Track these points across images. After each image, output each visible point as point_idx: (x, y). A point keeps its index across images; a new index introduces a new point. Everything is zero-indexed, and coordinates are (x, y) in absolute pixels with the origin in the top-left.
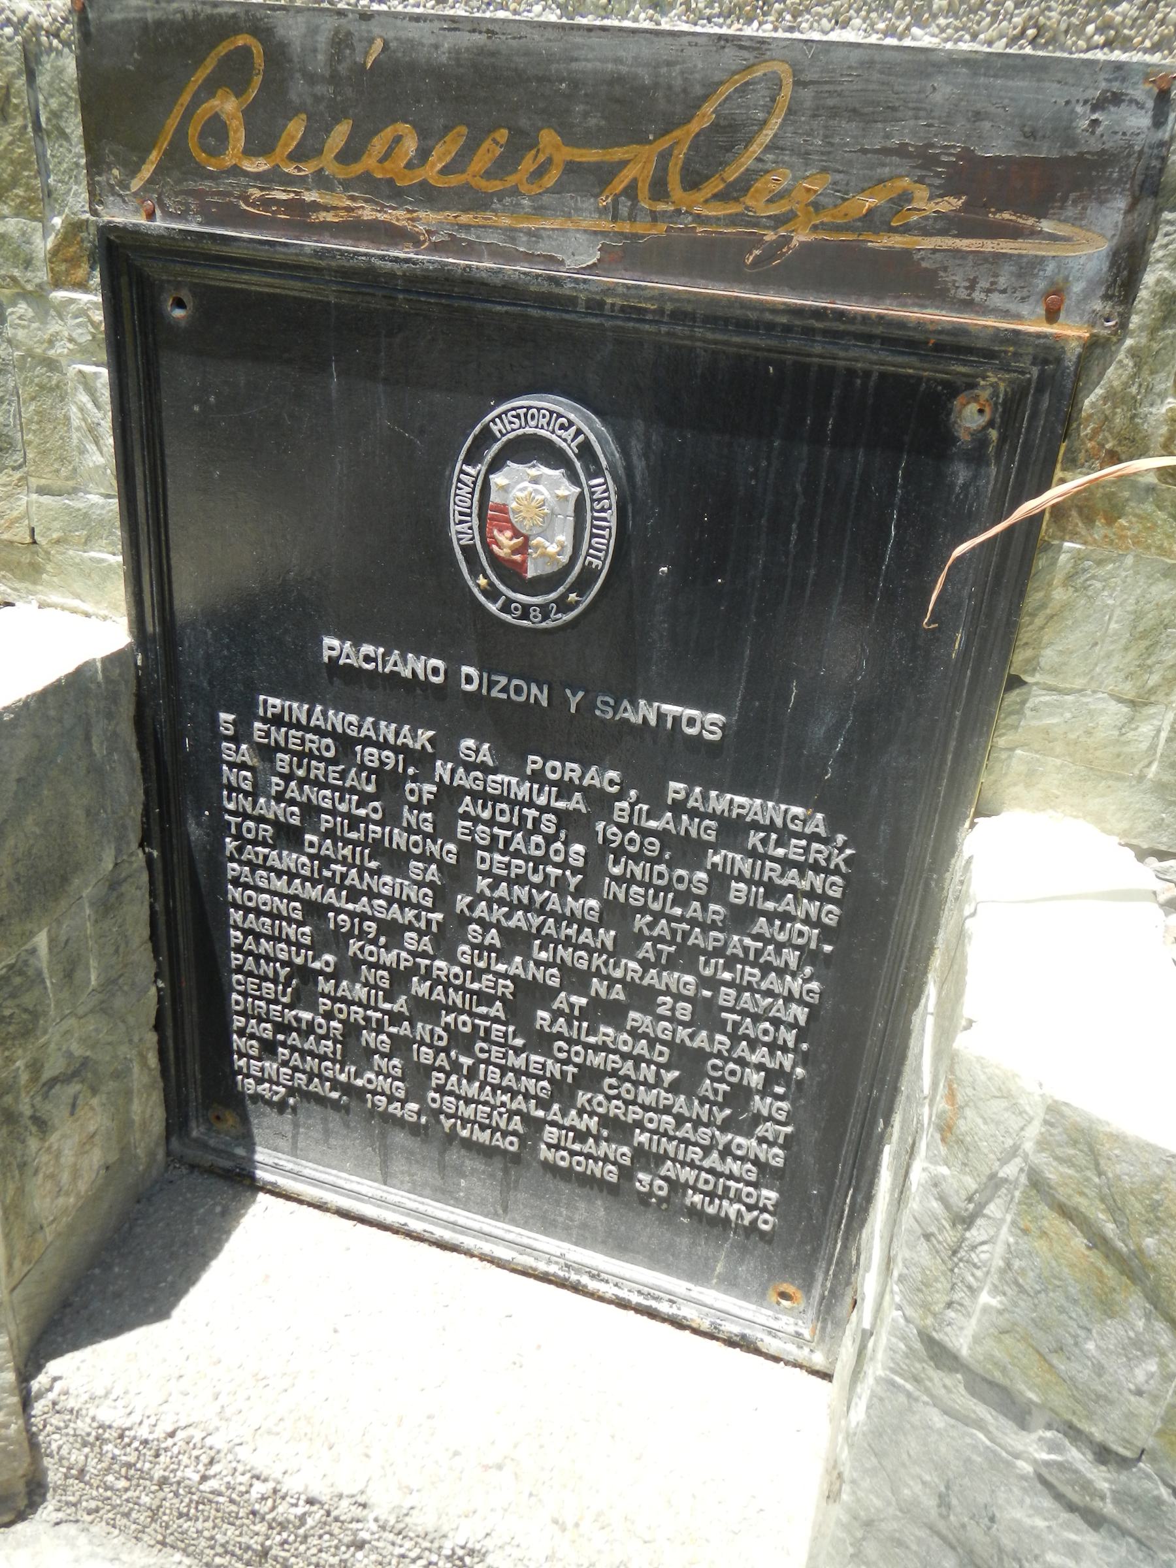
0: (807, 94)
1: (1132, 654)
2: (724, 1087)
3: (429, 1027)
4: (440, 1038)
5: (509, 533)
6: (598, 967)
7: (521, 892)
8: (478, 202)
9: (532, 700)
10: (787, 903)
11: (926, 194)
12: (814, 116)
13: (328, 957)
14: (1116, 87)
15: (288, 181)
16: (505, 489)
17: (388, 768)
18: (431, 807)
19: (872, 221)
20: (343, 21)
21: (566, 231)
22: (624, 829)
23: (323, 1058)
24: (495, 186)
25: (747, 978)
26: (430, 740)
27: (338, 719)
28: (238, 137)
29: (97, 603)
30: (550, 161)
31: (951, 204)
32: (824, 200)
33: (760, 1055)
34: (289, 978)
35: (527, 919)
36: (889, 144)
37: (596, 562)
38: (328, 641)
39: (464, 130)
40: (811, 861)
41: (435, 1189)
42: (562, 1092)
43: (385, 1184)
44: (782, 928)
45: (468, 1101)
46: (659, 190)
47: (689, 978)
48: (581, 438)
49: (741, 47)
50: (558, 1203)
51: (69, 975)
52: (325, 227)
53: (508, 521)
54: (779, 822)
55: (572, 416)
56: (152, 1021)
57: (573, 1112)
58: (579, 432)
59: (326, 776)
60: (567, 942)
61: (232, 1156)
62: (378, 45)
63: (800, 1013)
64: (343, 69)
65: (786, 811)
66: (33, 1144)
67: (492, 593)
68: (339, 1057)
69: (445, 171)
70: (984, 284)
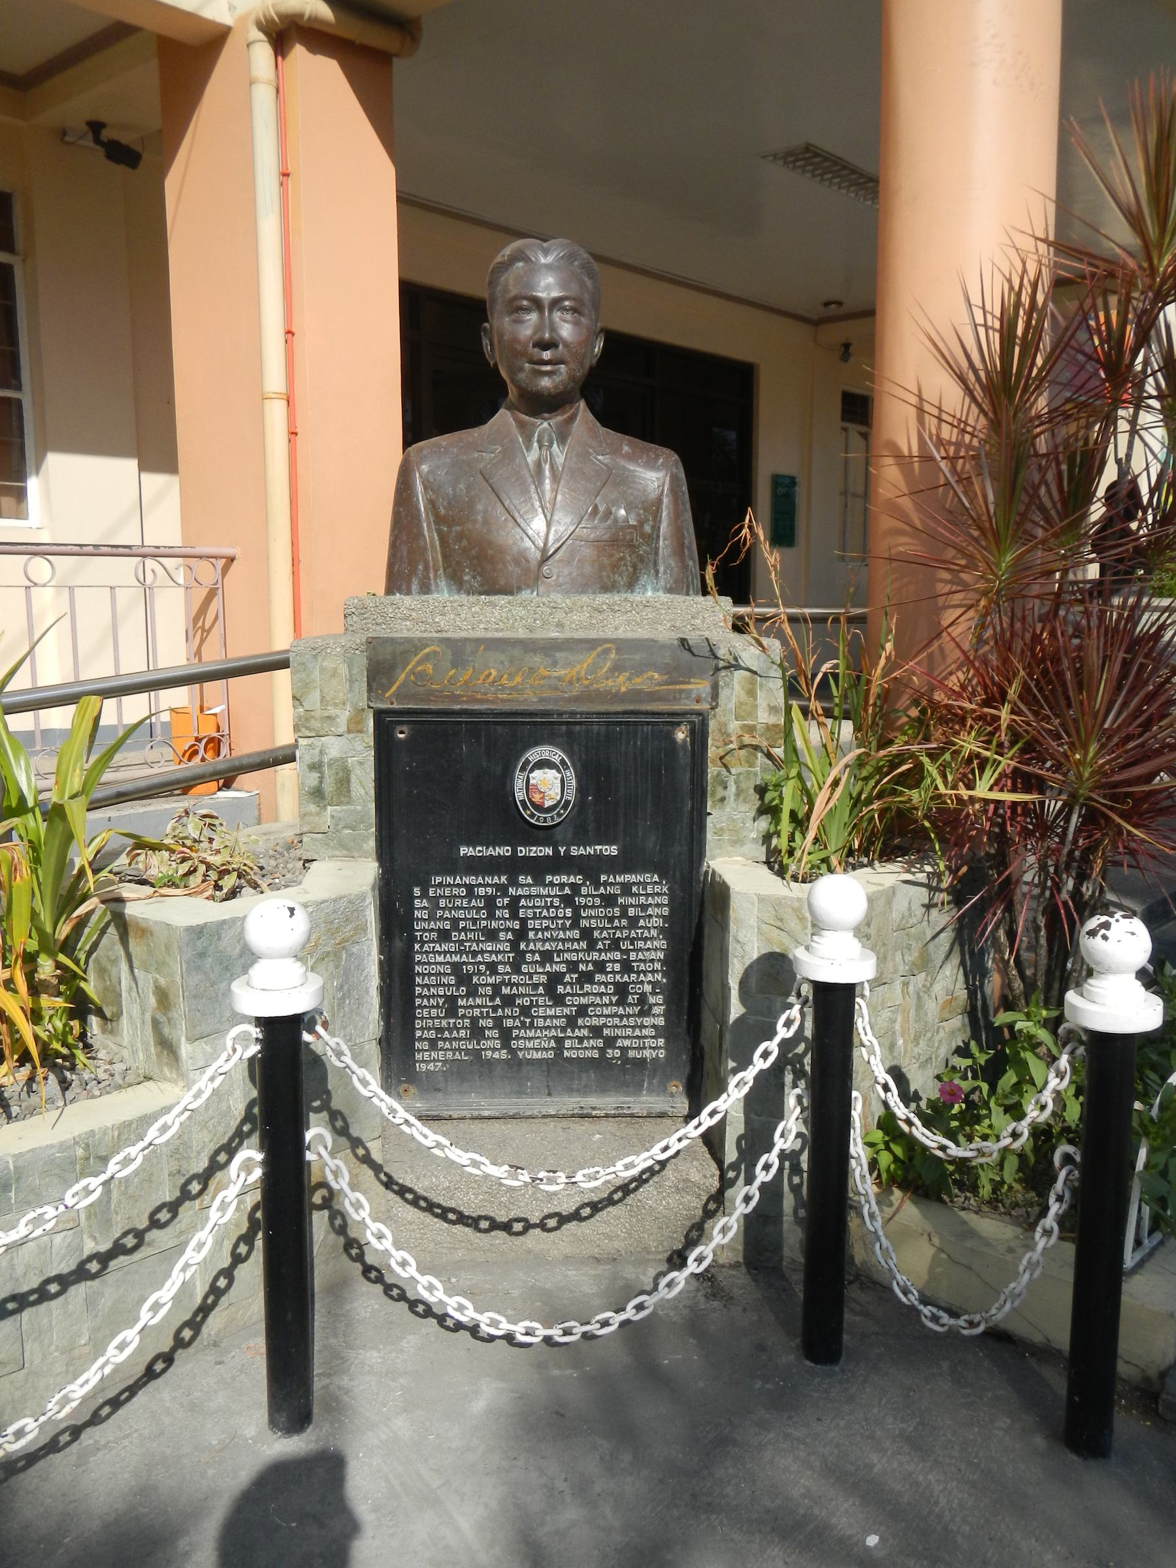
2: (636, 997)
7: (547, 934)
10: (650, 911)
18: (508, 906)
22: (585, 896)
23: (461, 1039)
27: (467, 880)
33: (650, 977)
42: (571, 1022)
45: (530, 1039)
50: (573, 1079)
60: (568, 950)
63: (661, 955)
67: (532, 816)
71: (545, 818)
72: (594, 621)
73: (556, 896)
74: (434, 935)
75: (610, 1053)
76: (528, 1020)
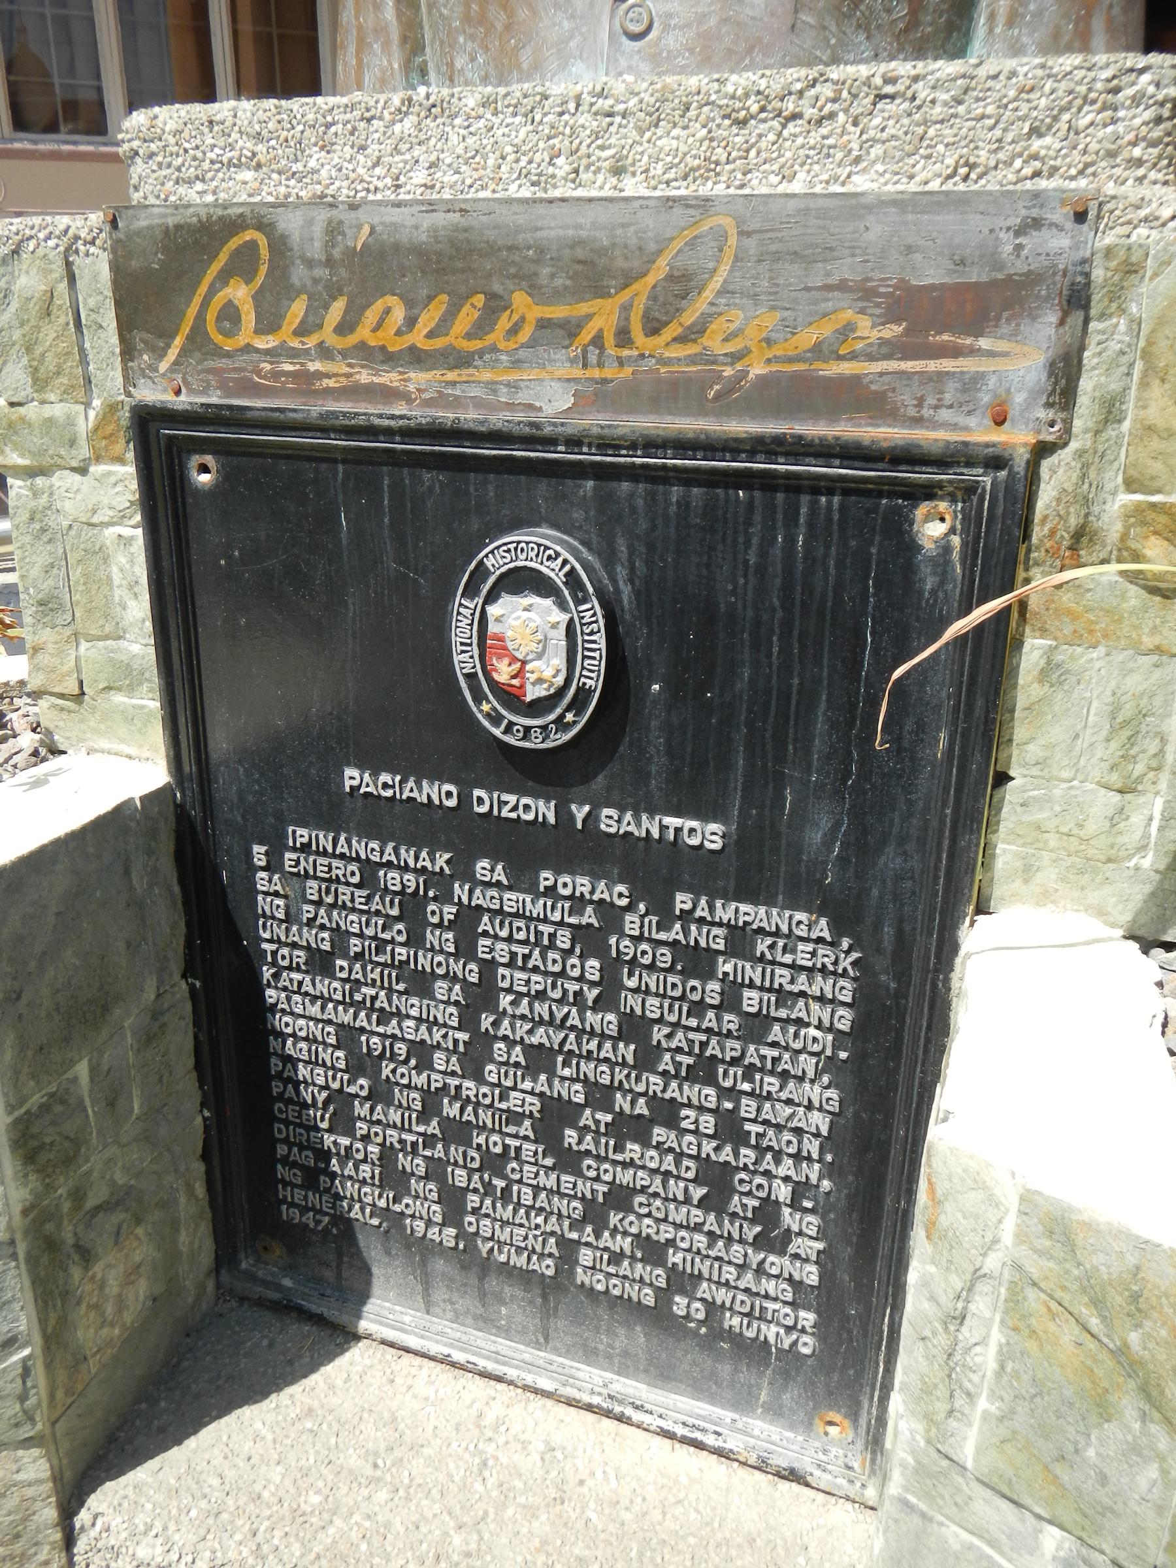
0: (751, 243)
1: (1114, 745)
3: (461, 1149)
4: (473, 1159)
5: (506, 661)
6: (621, 1082)
7: (542, 1009)
8: (463, 360)
9: (540, 819)
11: (869, 324)
12: (759, 261)
13: (362, 1081)
14: (1035, 213)
15: (293, 354)
16: (498, 620)
17: (409, 891)
19: (818, 351)
20: (334, 212)
21: (542, 380)
24: (475, 345)
25: (766, 1088)
26: (448, 862)
27: (359, 847)
28: (249, 319)
29: (140, 746)
30: (523, 319)
31: (893, 330)
32: (773, 335)
34: (326, 1103)
35: (548, 1037)
36: (830, 281)
37: (589, 682)
38: (349, 772)
39: (445, 297)
40: (819, 966)
41: (476, 1318)
43: (428, 1313)
44: (796, 1035)
45: (505, 1223)
46: (624, 337)
47: (710, 1091)
48: (567, 568)
49: (688, 206)
50: (597, 1329)
51: (111, 1104)
52: (328, 392)
53: (505, 648)
54: (784, 928)
55: (558, 548)
56: (199, 1151)
57: (606, 1234)
58: (565, 562)
59: (353, 901)
61: (278, 1287)
62: (366, 230)
64: (337, 253)
65: (791, 918)
66: (76, 1273)
67: (496, 719)
68: (377, 1182)
69: (430, 335)
70: (931, 400)
71: (527, 730)
72: (722, 156)
73: (561, 924)
74: (301, 956)
75: (680, 1304)
76: (499, 1183)
